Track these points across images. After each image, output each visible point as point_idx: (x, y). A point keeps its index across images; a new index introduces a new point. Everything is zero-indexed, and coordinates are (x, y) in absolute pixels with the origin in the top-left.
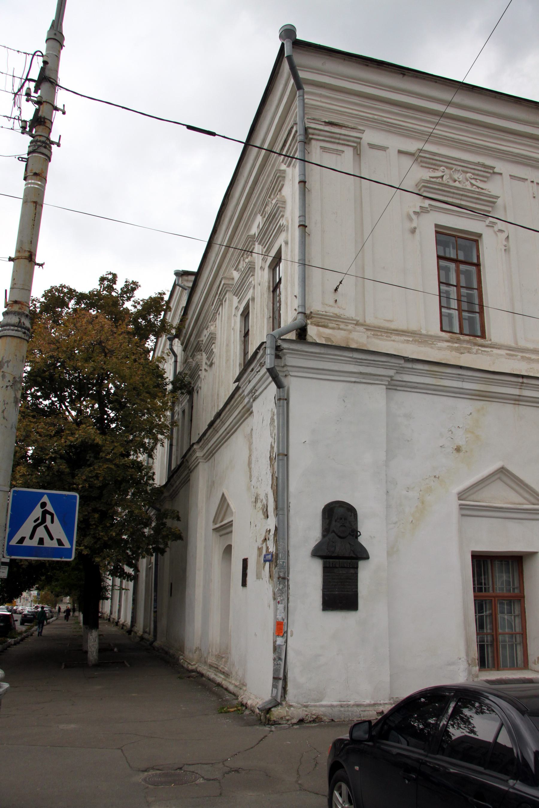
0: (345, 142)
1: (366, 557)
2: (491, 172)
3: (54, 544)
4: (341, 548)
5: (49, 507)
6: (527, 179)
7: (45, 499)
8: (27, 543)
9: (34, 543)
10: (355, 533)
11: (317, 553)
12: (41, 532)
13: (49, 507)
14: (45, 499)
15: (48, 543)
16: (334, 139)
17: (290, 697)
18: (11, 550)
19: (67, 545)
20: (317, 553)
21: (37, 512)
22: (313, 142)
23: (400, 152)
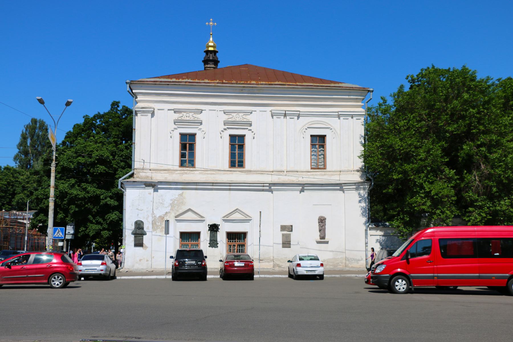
0: (148, 112)
1: (146, 234)
2: (201, 111)
3: (60, 236)
4: (138, 232)
5: (59, 230)
6: (215, 110)
7: (59, 229)
8: (56, 236)
9: (57, 236)
10: (143, 228)
11: (133, 234)
12: (58, 234)
13: (59, 230)
14: (59, 229)
15: (60, 236)
16: (144, 112)
17: (124, 267)
18: (54, 237)
19: (63, 236)
20: (133, 233)
21: (57, 231)
22: (138, 114)
23: (169, 110)
